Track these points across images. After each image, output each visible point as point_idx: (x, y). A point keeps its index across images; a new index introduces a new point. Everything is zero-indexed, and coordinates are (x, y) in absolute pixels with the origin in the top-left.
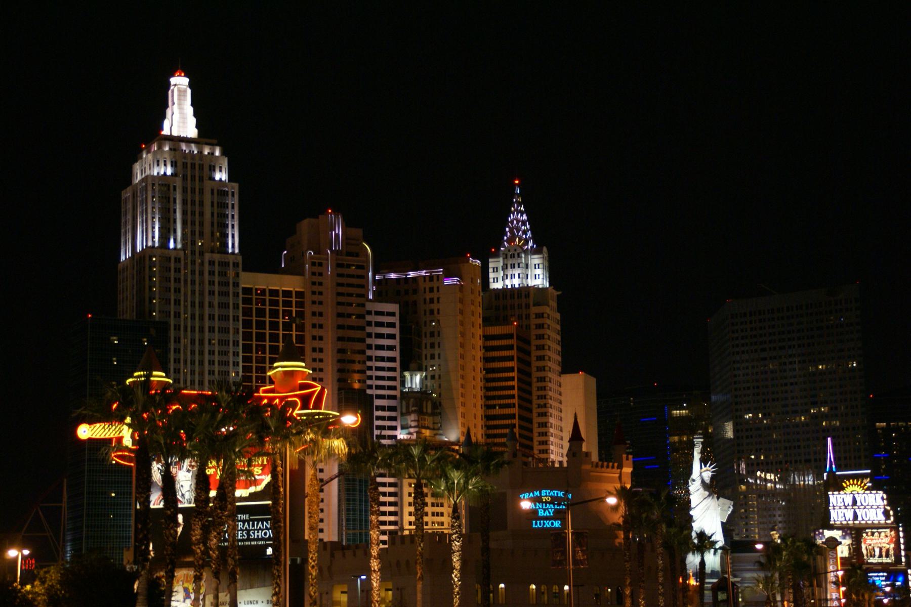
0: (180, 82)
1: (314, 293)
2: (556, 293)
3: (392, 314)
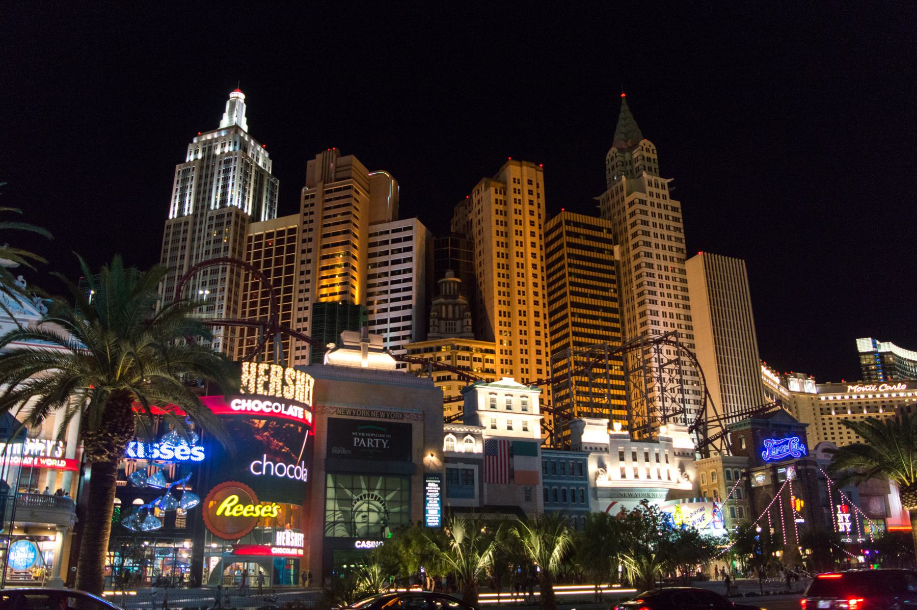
0: (238, 96)
1: (305, 223)
2: (666, 181)
3: (411, 228)
